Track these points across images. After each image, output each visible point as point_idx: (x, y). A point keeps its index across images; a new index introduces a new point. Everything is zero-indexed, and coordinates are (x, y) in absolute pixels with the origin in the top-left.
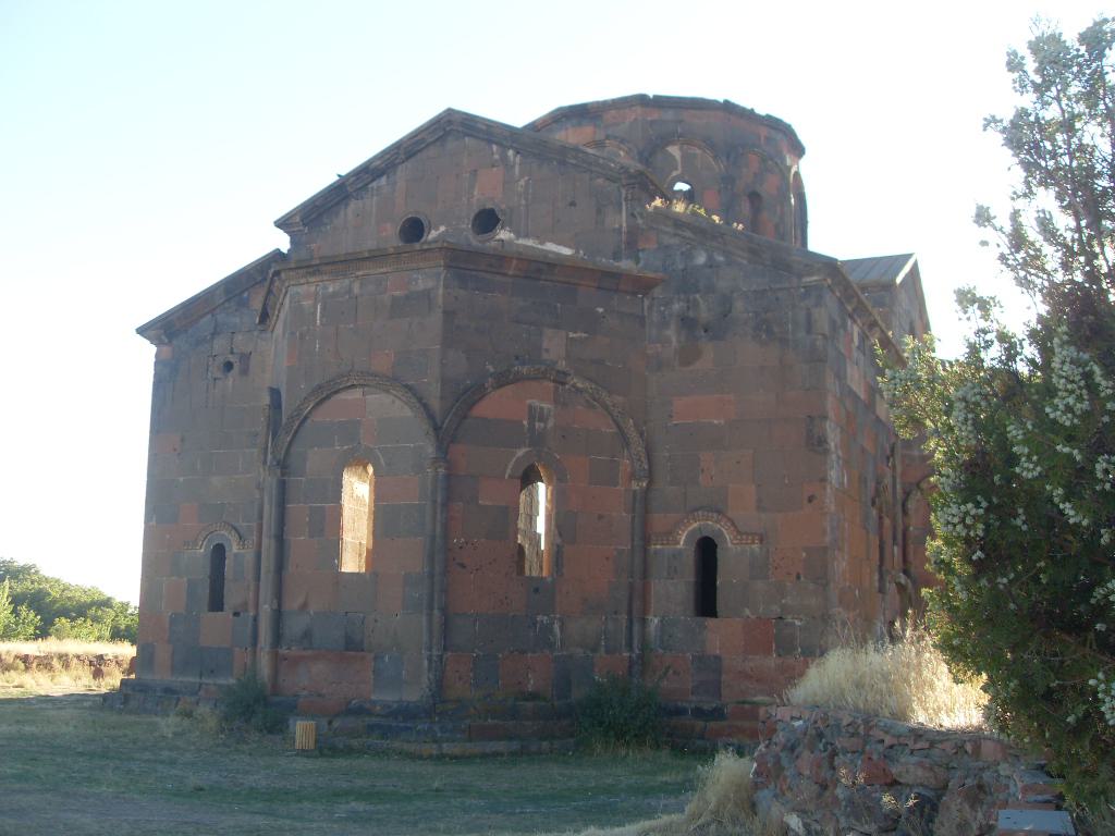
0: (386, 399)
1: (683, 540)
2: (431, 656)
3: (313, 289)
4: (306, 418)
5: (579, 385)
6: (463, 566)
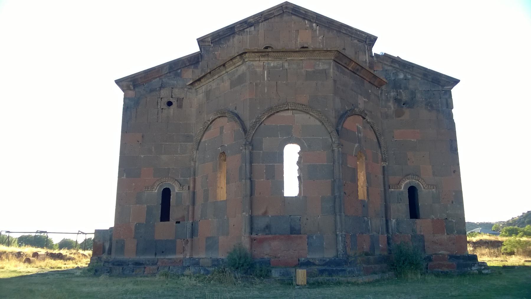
0: (306, 116)
1: (403, 188)
3: (262, 63)
4: (262, 123)
5: (368, 120)
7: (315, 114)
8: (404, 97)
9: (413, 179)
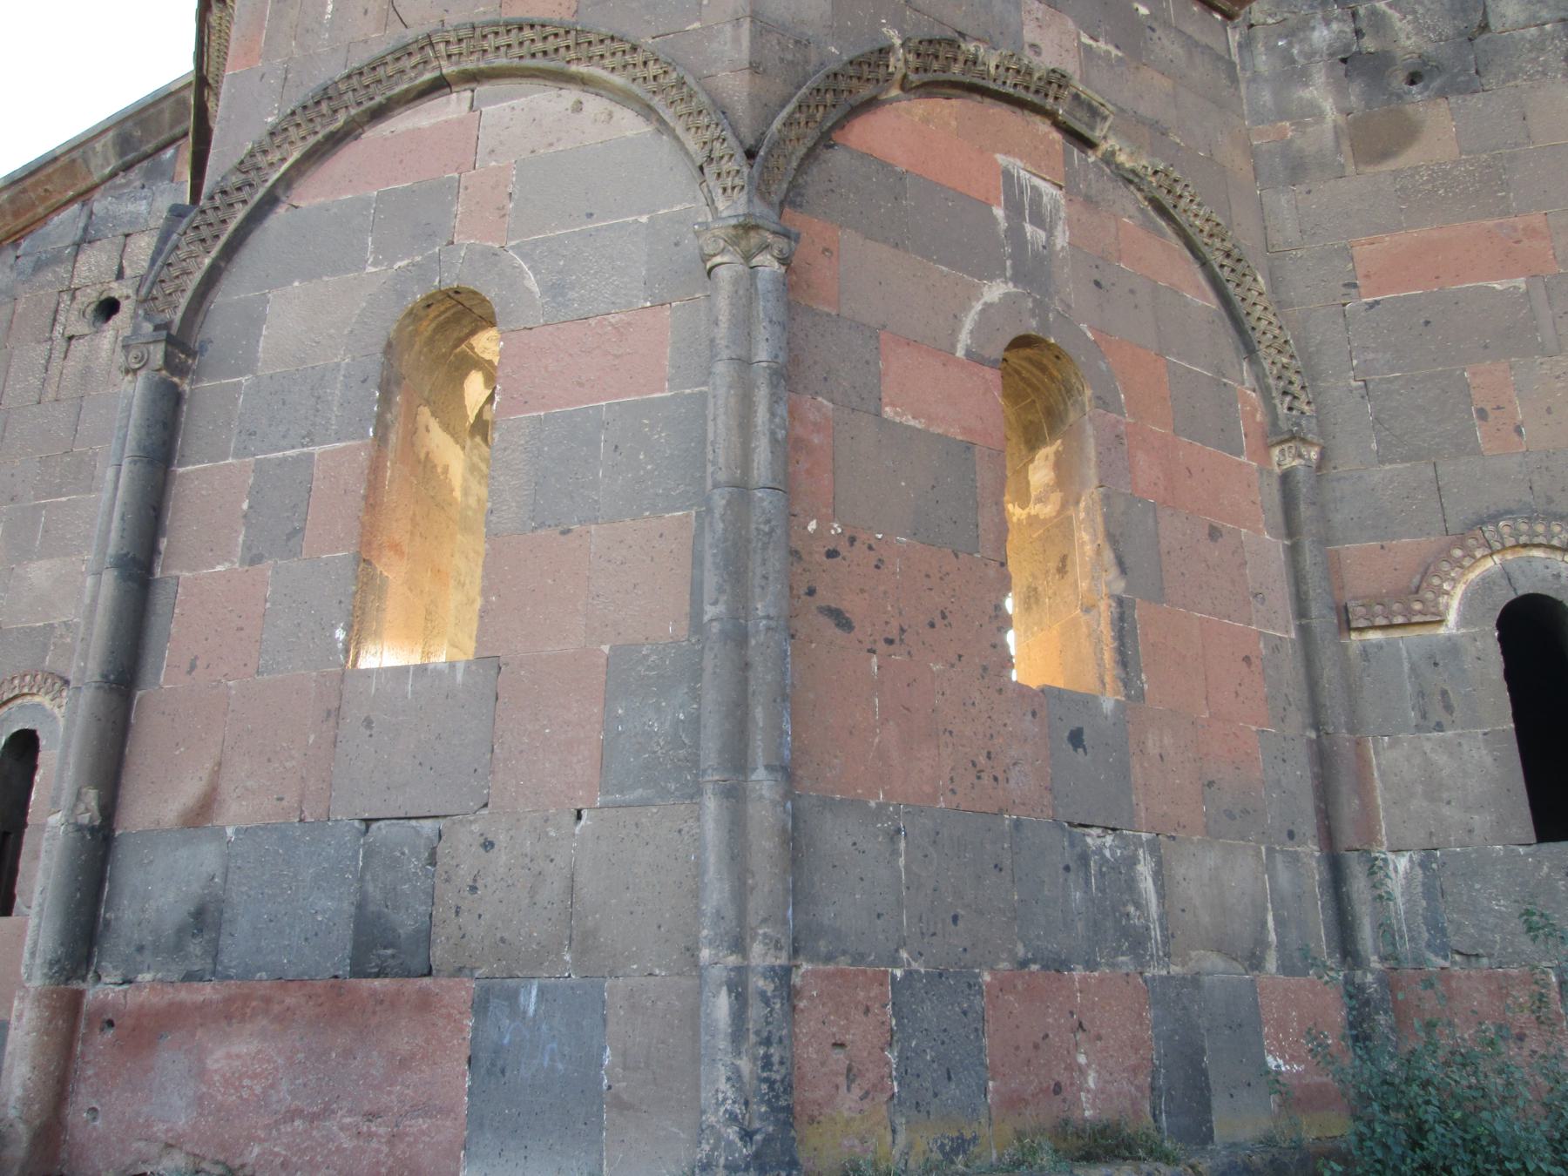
0: (550, 101)
2: (741, 971)
4: (270, 201)
5: (1122, 158)
6: (840, 619)
7: (604, 68)
8: (1408, 38)
9: (1525, 546)
